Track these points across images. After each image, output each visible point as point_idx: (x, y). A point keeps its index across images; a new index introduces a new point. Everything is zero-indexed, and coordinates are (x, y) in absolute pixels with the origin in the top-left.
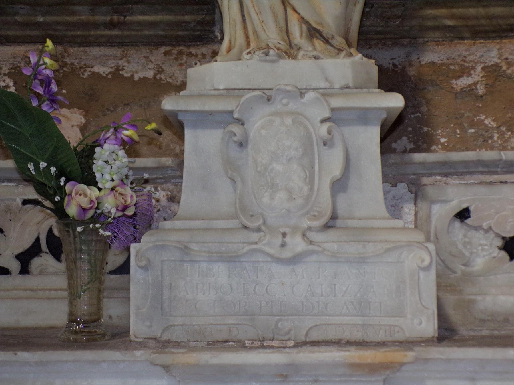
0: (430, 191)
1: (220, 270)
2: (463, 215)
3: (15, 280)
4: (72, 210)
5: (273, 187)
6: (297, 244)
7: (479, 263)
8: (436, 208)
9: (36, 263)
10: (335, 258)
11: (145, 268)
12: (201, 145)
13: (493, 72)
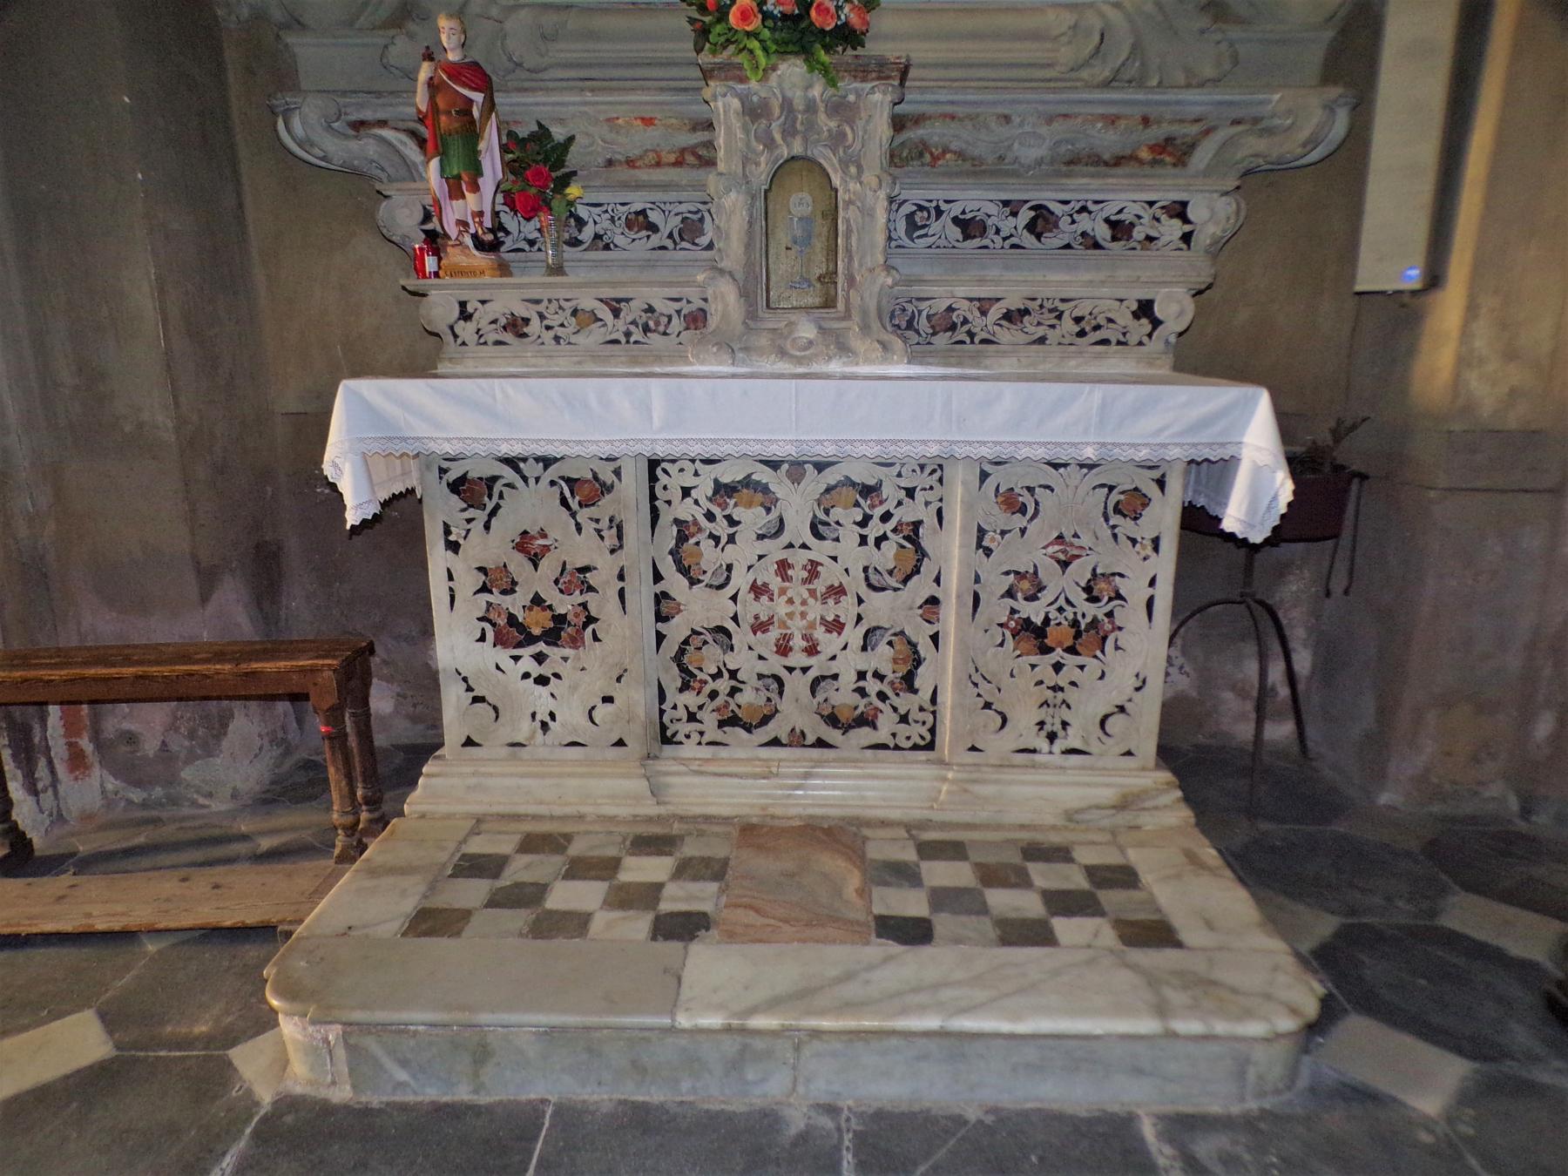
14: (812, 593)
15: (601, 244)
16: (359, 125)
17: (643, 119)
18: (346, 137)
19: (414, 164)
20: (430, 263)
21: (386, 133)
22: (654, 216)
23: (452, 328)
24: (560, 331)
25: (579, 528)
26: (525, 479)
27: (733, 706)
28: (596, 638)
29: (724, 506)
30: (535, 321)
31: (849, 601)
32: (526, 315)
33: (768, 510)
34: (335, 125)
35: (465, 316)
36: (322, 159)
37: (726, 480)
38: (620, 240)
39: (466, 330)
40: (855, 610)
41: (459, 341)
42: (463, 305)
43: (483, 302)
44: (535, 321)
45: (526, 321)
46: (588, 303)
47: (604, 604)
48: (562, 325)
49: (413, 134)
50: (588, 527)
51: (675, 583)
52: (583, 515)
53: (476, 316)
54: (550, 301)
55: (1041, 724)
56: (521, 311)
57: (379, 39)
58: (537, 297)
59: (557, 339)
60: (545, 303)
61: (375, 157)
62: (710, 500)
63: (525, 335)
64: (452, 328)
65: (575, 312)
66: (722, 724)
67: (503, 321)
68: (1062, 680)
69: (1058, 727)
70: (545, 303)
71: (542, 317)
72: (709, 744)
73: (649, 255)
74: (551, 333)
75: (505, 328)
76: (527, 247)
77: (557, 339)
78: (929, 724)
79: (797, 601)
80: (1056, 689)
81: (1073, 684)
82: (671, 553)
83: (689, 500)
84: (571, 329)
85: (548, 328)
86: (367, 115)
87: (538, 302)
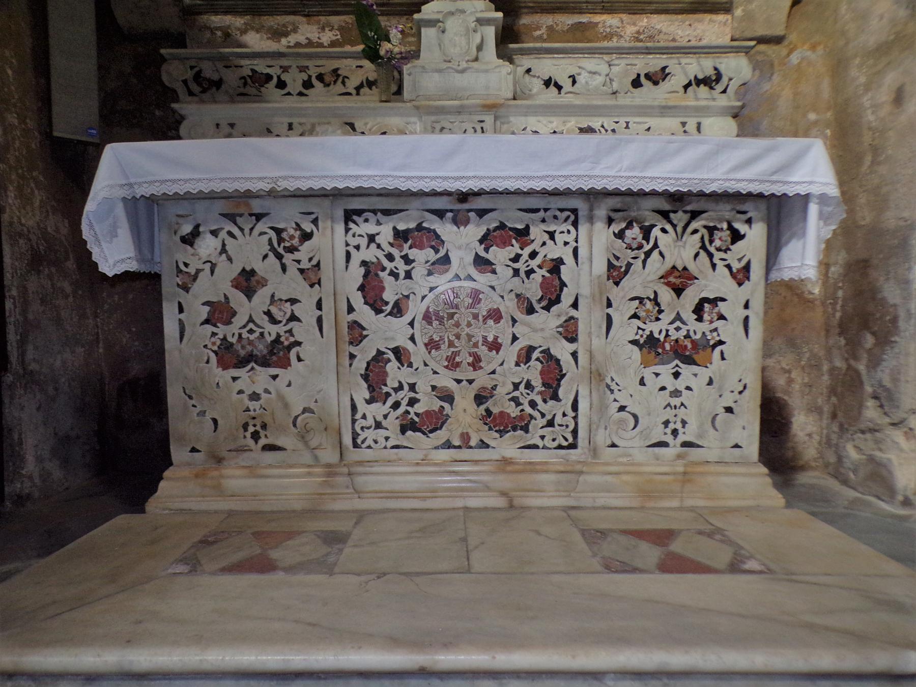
0: (516, 61)
1: (436, 76)
2: (529, 71)
3: (355, 98)
4: (382, 52)
5: (455, 46)
6: (464, 65)
7: (535, 91)
8: (519, 68)
9: (362, 91)
10: (477, 71)
11: (409, 75)
12: (428, 34)
13: (550, 29)
14: (476, 316)
25: (284, 268)
26: (242, 230)
27: (412, 415)
28: (299, 359)
29: (400, 248)
31: (505, 323)
33: (437, 251)
37: (401, 227)
40: (509, 331)
47: (304, 331)
50: (292, 269)
51: (364, 314)
52: (288, 258)
55: (666, 423)
62: (391, 245)
66: (403, 430)
68: (680, 384)
69: (679, 426)
72: (393, 447)
78: (572, 427)
79: (464, 324)
80: (676, 393)
81: (688, 388)
82: (362, 288)
83: (373, 246)
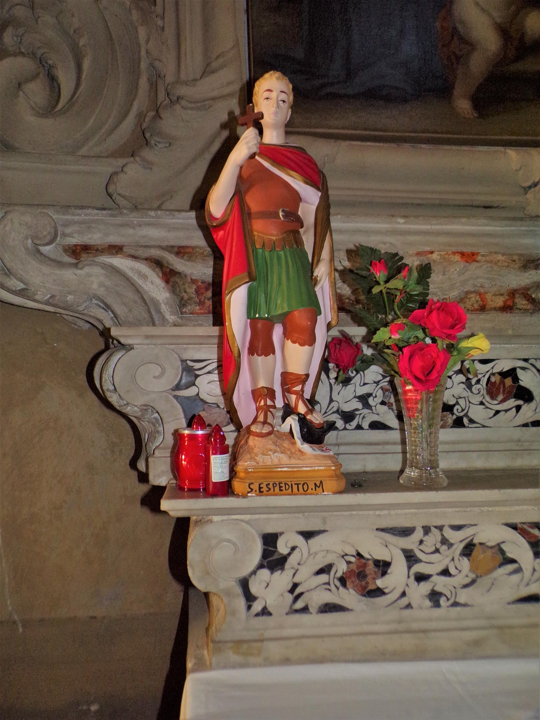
15: (450, 419)
16: (79, 252)
17: (462, 254)
18: (60, 264)
19: (156, 304)
20: (218, 468)
21: (118, 262)
22: (526, 379)
23: (244, 584)
24: (440, 583)
30: (399, 570)
32: (382, 555)
34: (45, 249)
35: (272, 560)
36: (21, 293)
38: (477, 413)
39: (272, 588)
41: (257, 607)
42: (270, 540)
43: (308, 535)
44: (399, 567)
45: (383, 567)
46: (491, 533)
48: (445, 572)
49: (157, 264)
53: (292, 561)
54: (427, 530)
56: (375, 548)
57: (106, 168)
58: (406, 523)
59: (435, 597)
60: (419, 534)
61: (101, 292)
63: (379, 592)
64: (244, 584)
65: (469, 550)
67: (341, 568)
70: (419, 534)
71: (411, 558)
73: (519, 433)
74: (425, 587)
75: (343, 581)
76: (340, 424)
77: (435, 597)
84: (459, 579)
85: (421, 578)
86: (94, 238)
87: (406, 532)
